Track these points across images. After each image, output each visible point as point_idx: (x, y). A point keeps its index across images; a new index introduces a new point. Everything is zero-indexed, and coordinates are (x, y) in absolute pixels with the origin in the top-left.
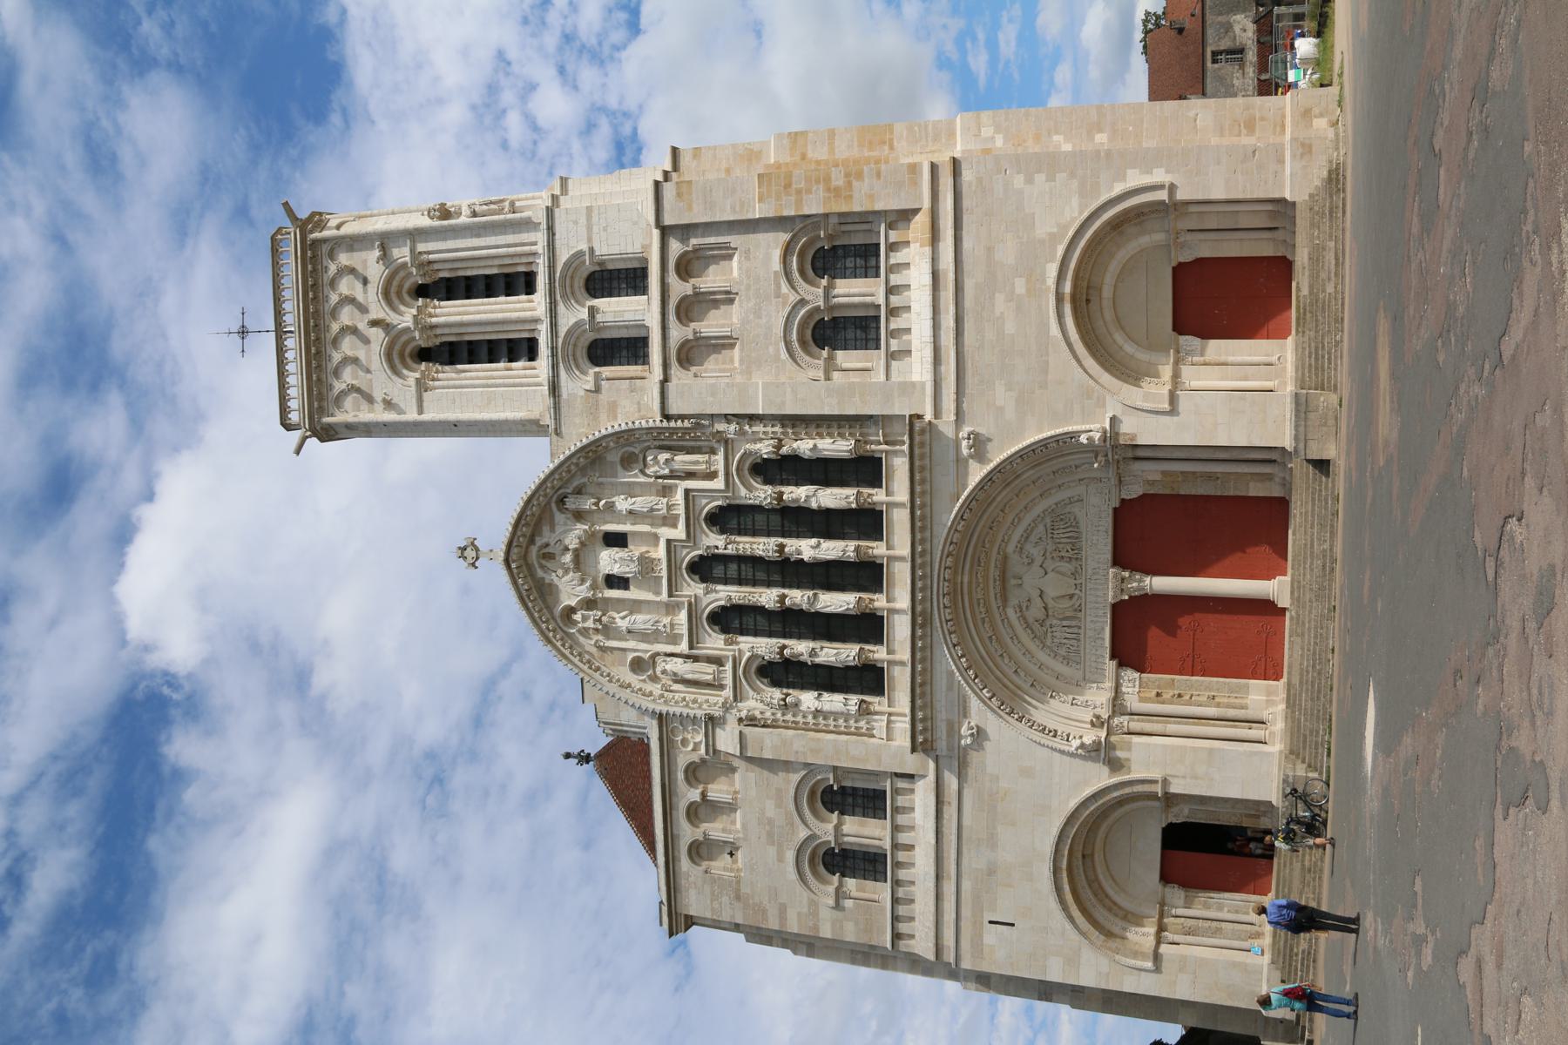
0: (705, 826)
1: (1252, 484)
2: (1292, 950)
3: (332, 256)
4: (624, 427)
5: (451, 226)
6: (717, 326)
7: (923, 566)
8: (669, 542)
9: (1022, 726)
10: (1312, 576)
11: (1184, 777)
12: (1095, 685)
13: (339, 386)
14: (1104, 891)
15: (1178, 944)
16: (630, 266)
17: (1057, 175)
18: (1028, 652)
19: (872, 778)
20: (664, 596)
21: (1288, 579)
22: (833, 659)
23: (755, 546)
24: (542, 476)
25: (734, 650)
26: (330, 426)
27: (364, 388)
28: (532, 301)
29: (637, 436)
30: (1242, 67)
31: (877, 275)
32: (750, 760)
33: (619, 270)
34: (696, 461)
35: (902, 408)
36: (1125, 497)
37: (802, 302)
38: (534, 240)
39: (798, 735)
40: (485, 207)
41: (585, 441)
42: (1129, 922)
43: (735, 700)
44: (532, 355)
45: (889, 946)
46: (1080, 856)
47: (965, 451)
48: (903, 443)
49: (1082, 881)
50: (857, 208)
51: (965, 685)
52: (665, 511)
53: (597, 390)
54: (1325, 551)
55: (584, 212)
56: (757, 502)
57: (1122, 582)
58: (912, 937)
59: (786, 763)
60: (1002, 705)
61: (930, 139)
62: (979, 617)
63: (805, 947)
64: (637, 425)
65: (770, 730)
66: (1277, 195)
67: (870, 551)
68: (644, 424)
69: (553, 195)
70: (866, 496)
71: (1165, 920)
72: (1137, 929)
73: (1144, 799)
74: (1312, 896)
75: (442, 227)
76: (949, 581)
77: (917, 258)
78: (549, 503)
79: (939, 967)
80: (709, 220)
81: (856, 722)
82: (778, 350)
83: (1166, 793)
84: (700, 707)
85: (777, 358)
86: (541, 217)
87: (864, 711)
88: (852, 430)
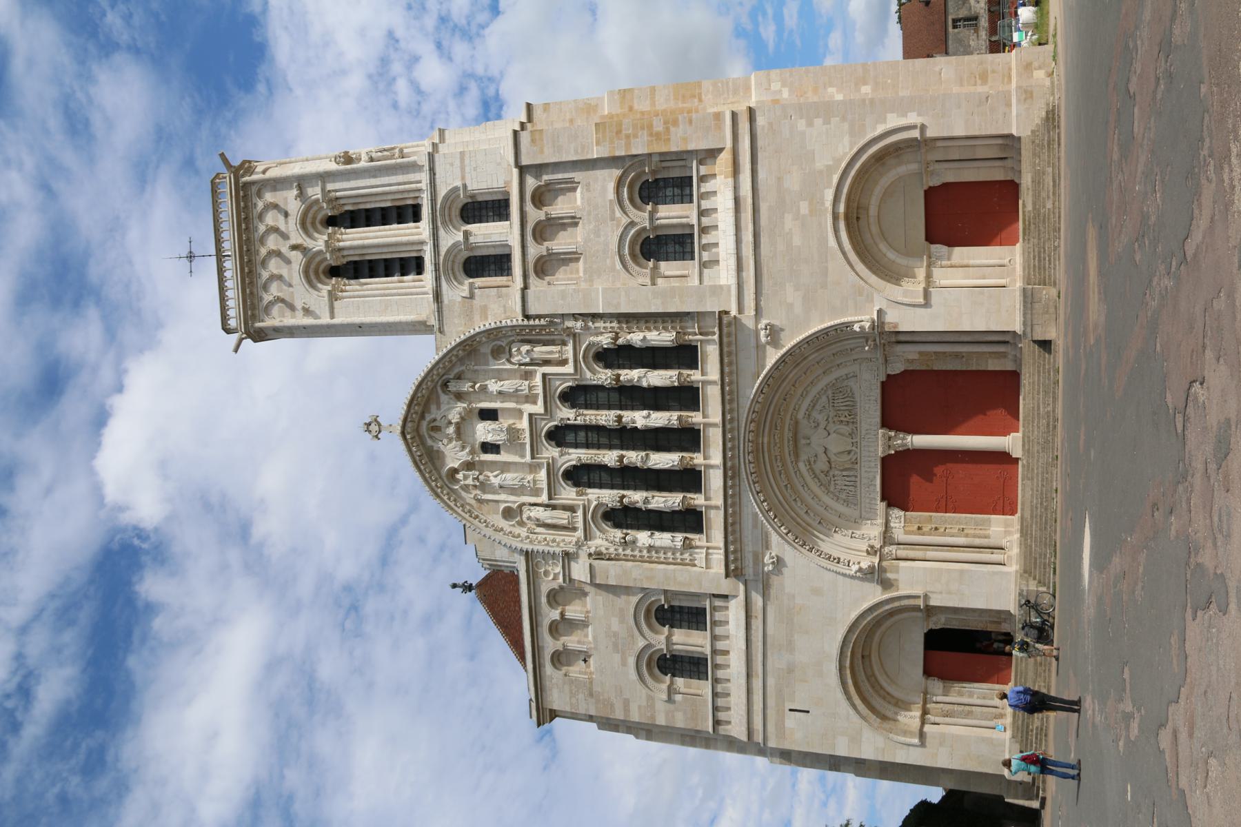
0: (564, 639)
1: (990, 361)
2: (1028, 727)
3: (259, 194)
4: (493, 325)
5: (353, 169)
6: (565, 244)
7: (731, 430)
8: (531, 415)
9: (812, 555)
10: (1038, 432)
11: (941, 593)
12: (869, 522)
13: (267, 298)
14: (879, 684)
15: (939, 724)
16: (495, 198)
18: (815, 496)
19: (695, 598)
20: (528, 458)
21: (1020, 435)
22: (662, 505)
23: (599, 418)
24: (430, 366)
25: (584, 500)
26: (261, 330)
27: (287, 299)
28: (418, 228)
29: (504, 332)
30: (976, 31)
31: (691, 201)
32: (599, 586)
33: (487, 202)
34: (551, 351)
35: (712, 306)
36: (890, 373)
37: (632, 224)
38: (419, 179)
39: (635, 566)
40: (380, 154)
41: (463, 337)
42: (899, 707)
43: (586, 539)
44: (419, 270)
45: (711, 730)
46: (860, 656)
47: (763, 339)
48: (714, 334)
49: (862, 677)
50: (674, 149)
51: (767, 524)
52: (527, 391)
53: (472, 296)
54: (1048, 412)
55: (458, 156)
56: (600, 383)
57: (889, 440)
58: (729, 723)
59: (627, 588)
60: (796, 539)
61: (730, 93)
62: (777, 470)
63: (644, 733)
64: (504, 324)
65: (613, 562)
66: (1006, 132)
67: (690, 419)
68: (509, 323)
69: (433, 143)
70: (685, 376)
71: (928, 706)
72: (906, 713)
73: (909, 611)
74: (1043, 684)
75: (346, 170)
76: (752, 442)
77: (722, 187)
78: (435, 387)
79: (751, 746)
80: (557, 161)
81: (681, 554)
83: (927, 606)
84: (558, 546)
85: (613, 269)
86: (424, 161)
87: (688, 546)
88: (673, 324)
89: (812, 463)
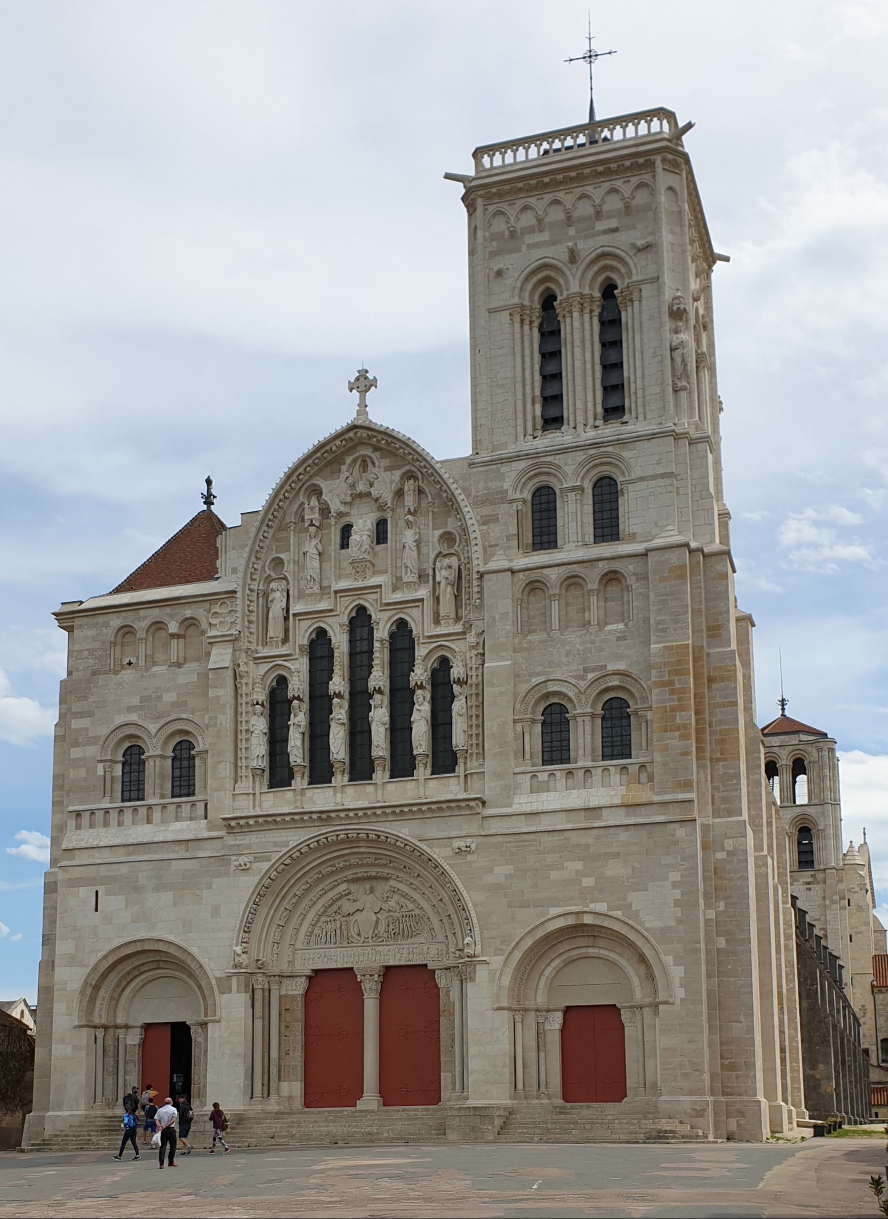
15: (96, 1043)
17: (680, 909)
34: (447, 606)
43: (256, 658)
57: (371, 975)
63: (63, 733)
82: (539, 675)
85: (532, 675)
89: (348, 897)
